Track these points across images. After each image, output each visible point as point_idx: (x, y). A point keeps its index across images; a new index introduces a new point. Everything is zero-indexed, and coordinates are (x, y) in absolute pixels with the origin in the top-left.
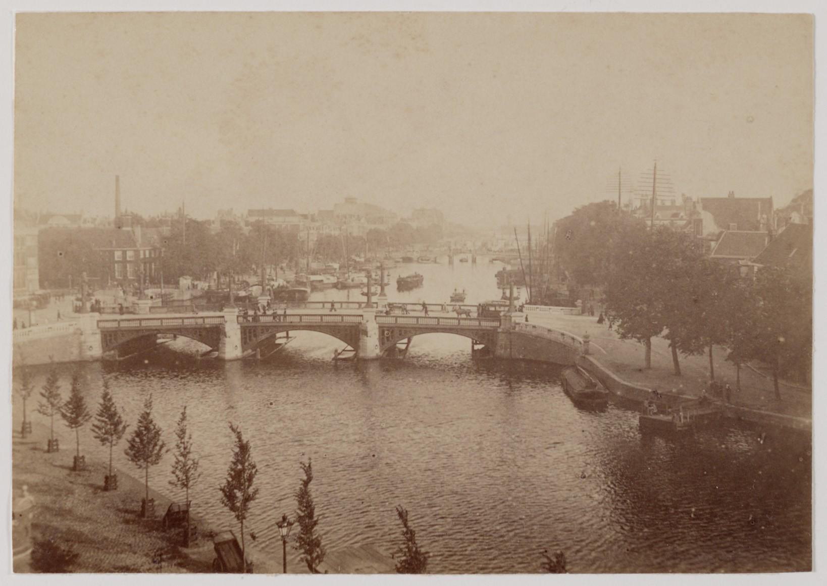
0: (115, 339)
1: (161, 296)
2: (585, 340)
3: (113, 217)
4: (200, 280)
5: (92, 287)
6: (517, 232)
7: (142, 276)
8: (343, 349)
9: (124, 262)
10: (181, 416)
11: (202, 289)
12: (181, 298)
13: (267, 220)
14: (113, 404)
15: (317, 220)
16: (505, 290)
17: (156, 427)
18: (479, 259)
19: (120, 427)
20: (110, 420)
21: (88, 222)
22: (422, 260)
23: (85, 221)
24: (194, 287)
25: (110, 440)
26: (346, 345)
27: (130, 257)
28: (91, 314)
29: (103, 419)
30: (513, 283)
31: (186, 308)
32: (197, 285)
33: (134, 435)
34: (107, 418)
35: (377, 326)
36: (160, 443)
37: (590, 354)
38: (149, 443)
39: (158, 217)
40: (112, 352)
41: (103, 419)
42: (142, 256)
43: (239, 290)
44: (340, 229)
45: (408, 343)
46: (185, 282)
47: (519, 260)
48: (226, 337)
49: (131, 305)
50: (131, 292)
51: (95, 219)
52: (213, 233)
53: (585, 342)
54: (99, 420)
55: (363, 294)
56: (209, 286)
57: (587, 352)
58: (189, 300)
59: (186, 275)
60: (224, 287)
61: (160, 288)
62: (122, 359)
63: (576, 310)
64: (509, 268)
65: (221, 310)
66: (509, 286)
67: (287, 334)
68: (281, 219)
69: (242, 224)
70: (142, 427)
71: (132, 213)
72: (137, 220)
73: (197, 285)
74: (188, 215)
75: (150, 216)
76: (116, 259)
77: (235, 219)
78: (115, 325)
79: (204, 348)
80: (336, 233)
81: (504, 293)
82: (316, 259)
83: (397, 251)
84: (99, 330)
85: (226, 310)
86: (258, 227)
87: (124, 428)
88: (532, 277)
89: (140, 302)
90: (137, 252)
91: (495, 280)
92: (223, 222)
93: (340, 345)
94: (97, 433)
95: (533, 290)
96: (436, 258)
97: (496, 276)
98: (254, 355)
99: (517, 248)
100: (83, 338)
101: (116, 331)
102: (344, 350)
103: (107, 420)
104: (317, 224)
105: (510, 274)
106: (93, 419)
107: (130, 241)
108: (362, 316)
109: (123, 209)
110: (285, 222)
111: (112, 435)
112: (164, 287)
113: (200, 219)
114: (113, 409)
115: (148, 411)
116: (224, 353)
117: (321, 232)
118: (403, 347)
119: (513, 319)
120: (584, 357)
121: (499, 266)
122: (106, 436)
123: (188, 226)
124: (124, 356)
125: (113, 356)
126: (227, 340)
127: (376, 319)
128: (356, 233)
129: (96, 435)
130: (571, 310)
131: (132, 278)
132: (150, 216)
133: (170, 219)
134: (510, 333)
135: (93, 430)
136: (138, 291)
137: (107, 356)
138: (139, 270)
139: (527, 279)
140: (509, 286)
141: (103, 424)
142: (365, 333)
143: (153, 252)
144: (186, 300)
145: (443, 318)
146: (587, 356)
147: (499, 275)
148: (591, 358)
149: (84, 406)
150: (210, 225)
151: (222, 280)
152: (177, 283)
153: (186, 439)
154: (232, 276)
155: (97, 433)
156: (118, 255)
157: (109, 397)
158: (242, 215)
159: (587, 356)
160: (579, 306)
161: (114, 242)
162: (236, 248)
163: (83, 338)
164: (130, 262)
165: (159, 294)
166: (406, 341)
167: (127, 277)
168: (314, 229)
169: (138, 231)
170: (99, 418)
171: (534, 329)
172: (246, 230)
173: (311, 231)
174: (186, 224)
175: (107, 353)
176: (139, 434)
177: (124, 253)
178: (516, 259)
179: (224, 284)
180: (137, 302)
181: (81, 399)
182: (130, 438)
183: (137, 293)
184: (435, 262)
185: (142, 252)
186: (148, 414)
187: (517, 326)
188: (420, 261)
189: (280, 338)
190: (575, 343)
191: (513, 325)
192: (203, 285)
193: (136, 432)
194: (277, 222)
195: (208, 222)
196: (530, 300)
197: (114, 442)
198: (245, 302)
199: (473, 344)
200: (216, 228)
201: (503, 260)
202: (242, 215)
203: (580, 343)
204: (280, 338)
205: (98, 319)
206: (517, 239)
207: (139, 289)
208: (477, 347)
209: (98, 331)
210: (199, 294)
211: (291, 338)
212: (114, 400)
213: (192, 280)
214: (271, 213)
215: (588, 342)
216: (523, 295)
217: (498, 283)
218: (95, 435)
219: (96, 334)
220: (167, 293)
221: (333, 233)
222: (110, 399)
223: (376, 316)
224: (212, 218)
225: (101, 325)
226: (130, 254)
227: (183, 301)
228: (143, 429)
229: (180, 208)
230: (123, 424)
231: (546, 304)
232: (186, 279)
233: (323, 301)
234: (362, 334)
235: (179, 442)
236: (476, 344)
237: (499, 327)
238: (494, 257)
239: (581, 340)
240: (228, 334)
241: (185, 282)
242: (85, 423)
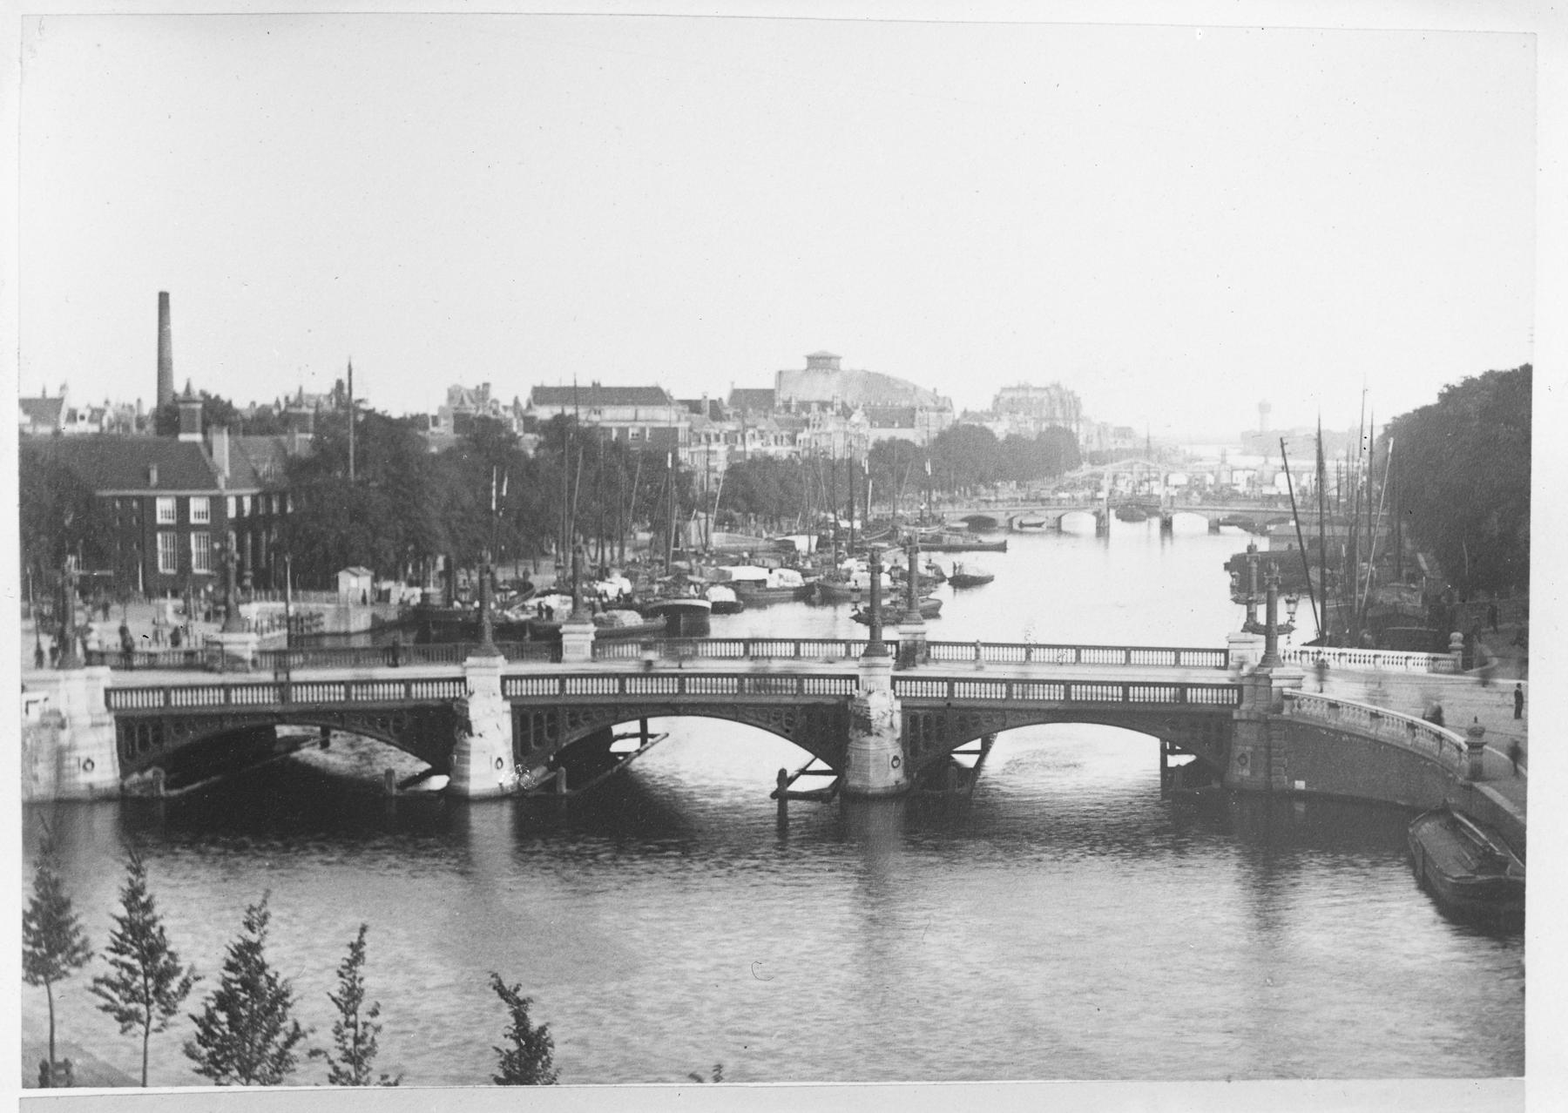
0: (158, 739)
1: (287, 621)
2: (1476, 740)
3: (150, 404)
4: (396, 579)
5: (91, 598)
6: (1287, 448)
7: (232, 566)
8: (802, 767)
9: (182, 526)
10: (348, 954)
11: (401, 602)
12: (343, 628)
13: (585, 416)
14: (154, 920)
15: (728, 415)
16: (1254, 605)
17: (279, 983)
18: (1180, 521)
19: (174, 985)
20: (144, 963)
21: (82, 418)
22: (1021, 525)
23: (73, 416)
24: (383, 597)
25: (144, 1018)
26: (810, 756)
27: (198, 515)
28: (88, 671)
29: (126, 959)
30: (1275, 589)
31: (355, 656)
32: (388, 592)
33: (212, 1004)
34: (134, 957)
35: (898, 705)
36: (288, 1025)
37: (1484, 780)
38: (254, 1024)
39: (278, 404)
40: (149, 774)
41: (126, 959)
42: (232, 513)
43: (506, 605)
44: (793, 441)
45: (983, 753)
46: (354, 583)
47: (1293, 523)
48: (471, 734)
49: (200, 646)
50: (201, 610)
51: (102, 412)
52: (434, 450)
53: (1471, 746)
54: (114, 963)
55: (857, 618)
56: (424, 596)
57: (1477, 773)
58: (365, 632)
59: (356, 565)
60: (464, 597)
61: (284, 598)
62: (175, 792)
63: (1447, 660)
64: (1263, 545)
65: (455, 657)
66: (1264, 596)
67: (644, 726)
68: (627, 412)
69: (516, 427)
70: (236, 982)
71: (203, 393)
72: (217, 413)
73: (388, 592)
74: (360, 401)
75: (253, 403)
76: (160, 520)
77: (495, 412)
78: (157, 700)
79: (407, 764)
80: (782, 451)
81: (1251, 615)
82: (724, 522)
83: (952, 501)
84: (113, 714)
85: (470, 660)
86: (558, 430)
87: (186, 987)
88: (1328, 571)
89: (226, 637)
90: (217, 504)
91: (1227, 579)
92: (462, 422)
93: (794, 756)
94: (107, 997)
95: (1330, 604)
96: (1060, 518)
97: (1227, 566)
98: (549, 785)
99: (1286, 491)
100: (64, 737)
101: (160, 718)
102: (803, 772)
103: (136, 963)
104: (730, 426)
105: (1265, 560)
106: (96, 960)
107: (197, 472)
109: (179, 387)
110: (635, 420)
111: (148, 1003)
112: (295, 598)
113: (396, 413)
114: (154, 930)
115: (254, 938)
116: (467, 778)
117: (739, 448)
118: (969, 761)
119: (1275, 683)
120: (1471, 788)
121: (1237, 541)
122: (133, 1006)
123: (361, 429)
124: (180, 786)
125: (151, 785)
126: (474, 743)
127: (893, 687)
128: (838, 450)
129: (108, 1002)
130: (1435, 659)
131: (204, 571)
132: (253, 403)
133: (311, 411)
134: (1267, 723)
135: (95, 990)
136: (222, 608)
137: (134, 786)
138: (224, 550)
139: (1315, 575)
140: (1264, 596)
141: (125, 973)
142: (866, 725)
143: (261, 500)
144: (358, 633)
145: (1081, 683)
146: (1476, 785)
147: (1237, 565)
148: (1488, 790)
149: (72, 928)
150: (426, 428)
151: (462, 577)
152: (331, 585)
153: (362, 1015)
154: (488, 571)
155: (107, 997)
156: (164, 507)
157: (143, 899)
158: (516, 402)
159: (1476, 785)
160: (1457, 649)
161: (154, 475)
162: (499, 490)
163: (64, 737)
164: (197, 528)
165: (280, 617)
166: (976, 745)
167: (190, 569)
168: (717, 438)
169: (222, 443)
170: (117, 956)
171: (1332, 711)
172: (529, 443)
173: (713, 447)
174: (357, 425)
175: (135, 777)
176: (225, 1000)
177: (183, 506)
178: (1282, 520)
179: (464, 591)
180: (218, 637)
181: (65, 905)
182: (200, 1012)
183: (218, 614)
184: (1057, 529)
185: (232, 502)
186: (255, 948)
187: (1287, 703)
188: (1016, 527)
189: (624, 737)
190: (1445, 749)
191: (1274, 701)
192: (403, 593)
193: (219, 995)
194: (613, 417)
195: (419, 421)
196: (1321, 633)
197: (154, 1024)
198: (521, 638)
199: (1165, 753)
200: (443, 435)
201: (1247, 526)
202: (516, 402)
203: (1459, 748)
204: (624, 737)
205: (109, 684)
206: (1285, 468)
207: (225, 602)
208: (1173, 761)
209: (109, 718)
210: (392, 615)
211: (653, 736)
212: (157, 911)
213: (375, 579)
214: (599, 395)
215: (1480, 746)
216: (1304, 619)
217: (1232, 587)
218: (103, 1001)
219: (102, 725)
220: (304, 613)
221: (772, 450)
222: (148, 907)
223: (894, 679)
224: (433, 411)
225: (118, 700)
226: (198, 506)
227: (347, 634)
228: (239, 986)
229: (340, 384)
230: (184, 973)
231: (1363, 645)
232: (357, 575)
233: (746, 635)
234: (856, 728)
235: (342, 1021)
236: (1173, 752)
238: (1222, 516)
239: (1460, 740)
240: (475, 730)
241: (353, 582)
242: (74, 971)
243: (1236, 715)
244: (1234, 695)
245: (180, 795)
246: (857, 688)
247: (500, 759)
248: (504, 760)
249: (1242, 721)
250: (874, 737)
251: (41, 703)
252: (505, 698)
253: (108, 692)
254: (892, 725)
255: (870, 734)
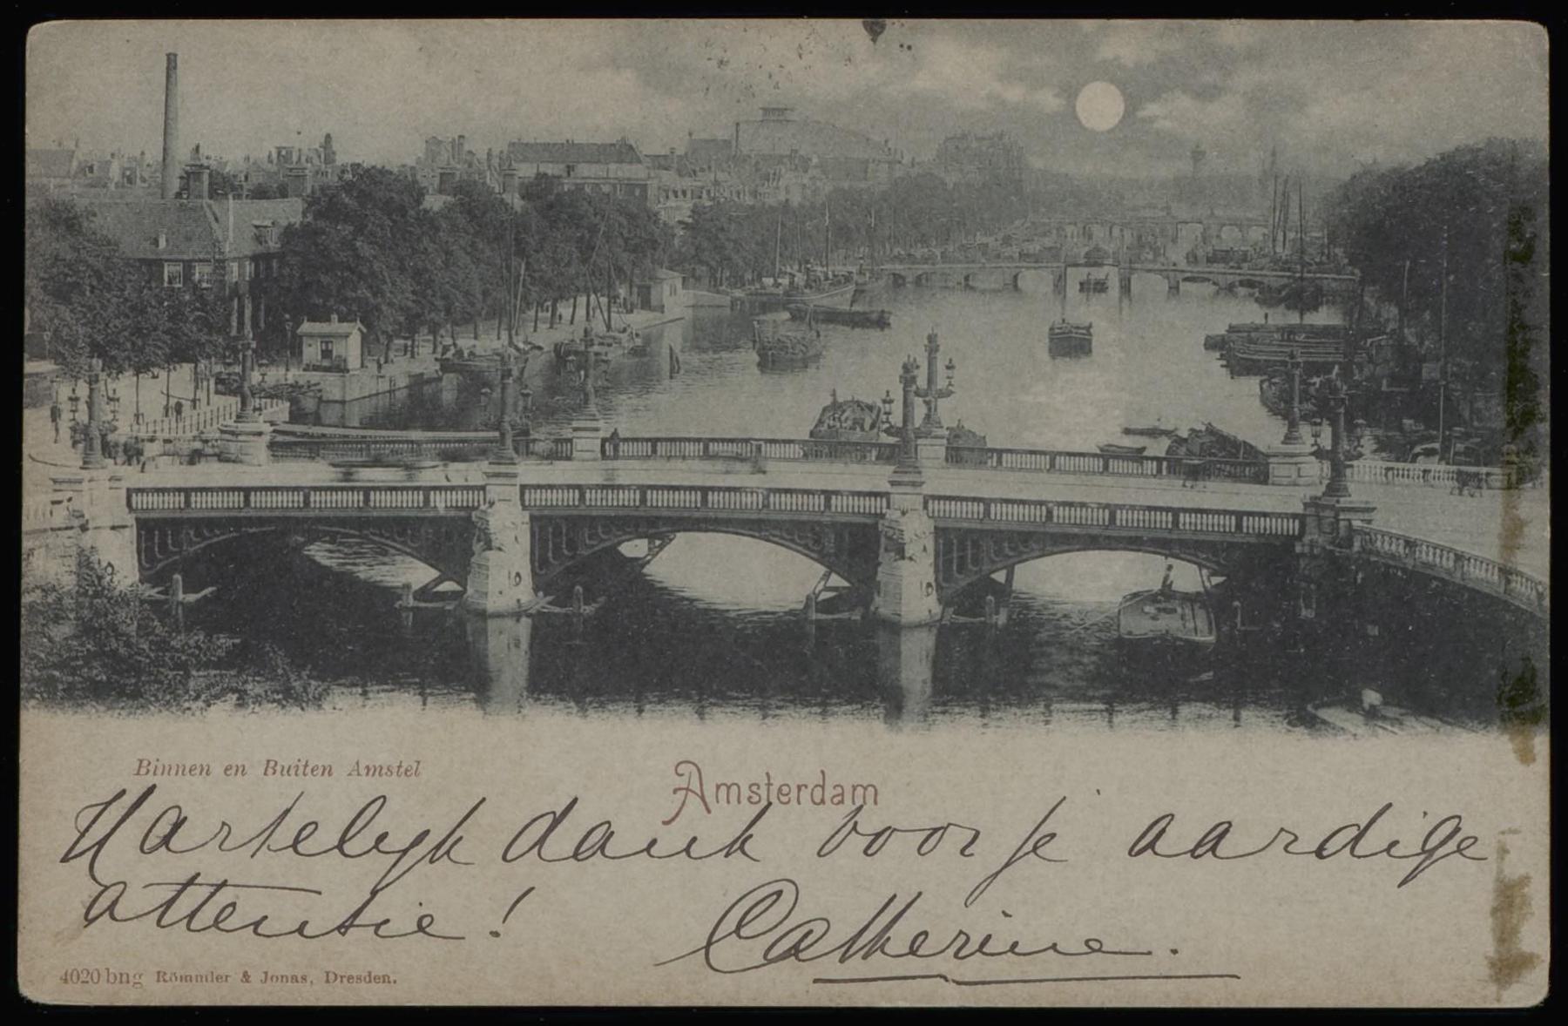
62: (192, 598)
100: (87, 540)
108: (886, 495)
127: (926, 507)
163: (87, 540)
209: (130, 520)
237: (1300, 537)
243: (1298, 549)
244: (1293, 527)
245: (198, 601)
246: (888, 507)
247: (518, 575)
248: (522, 575)
249: (1303, 555)
250: (906, 561)
251: (65, 503)
252: (524, 507)
253: (129, 492)
254: (925, 549)
255: (903, 558)
